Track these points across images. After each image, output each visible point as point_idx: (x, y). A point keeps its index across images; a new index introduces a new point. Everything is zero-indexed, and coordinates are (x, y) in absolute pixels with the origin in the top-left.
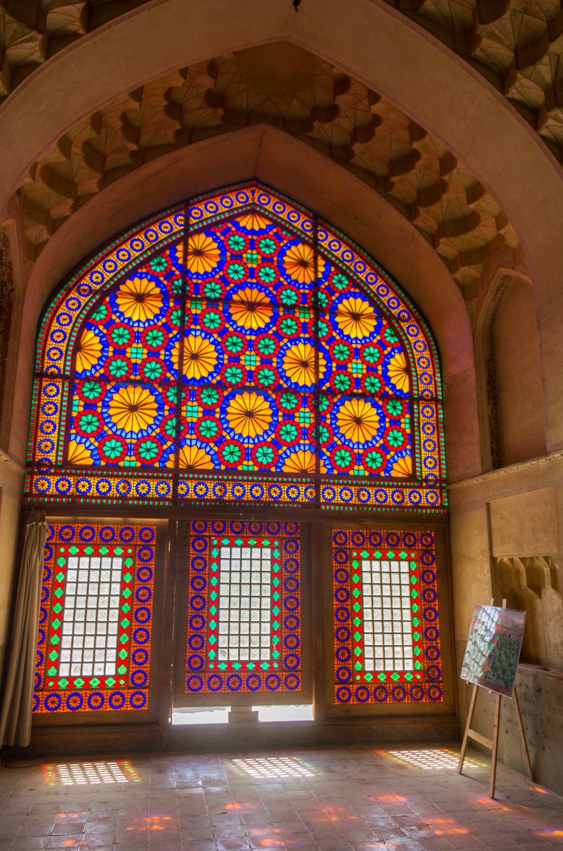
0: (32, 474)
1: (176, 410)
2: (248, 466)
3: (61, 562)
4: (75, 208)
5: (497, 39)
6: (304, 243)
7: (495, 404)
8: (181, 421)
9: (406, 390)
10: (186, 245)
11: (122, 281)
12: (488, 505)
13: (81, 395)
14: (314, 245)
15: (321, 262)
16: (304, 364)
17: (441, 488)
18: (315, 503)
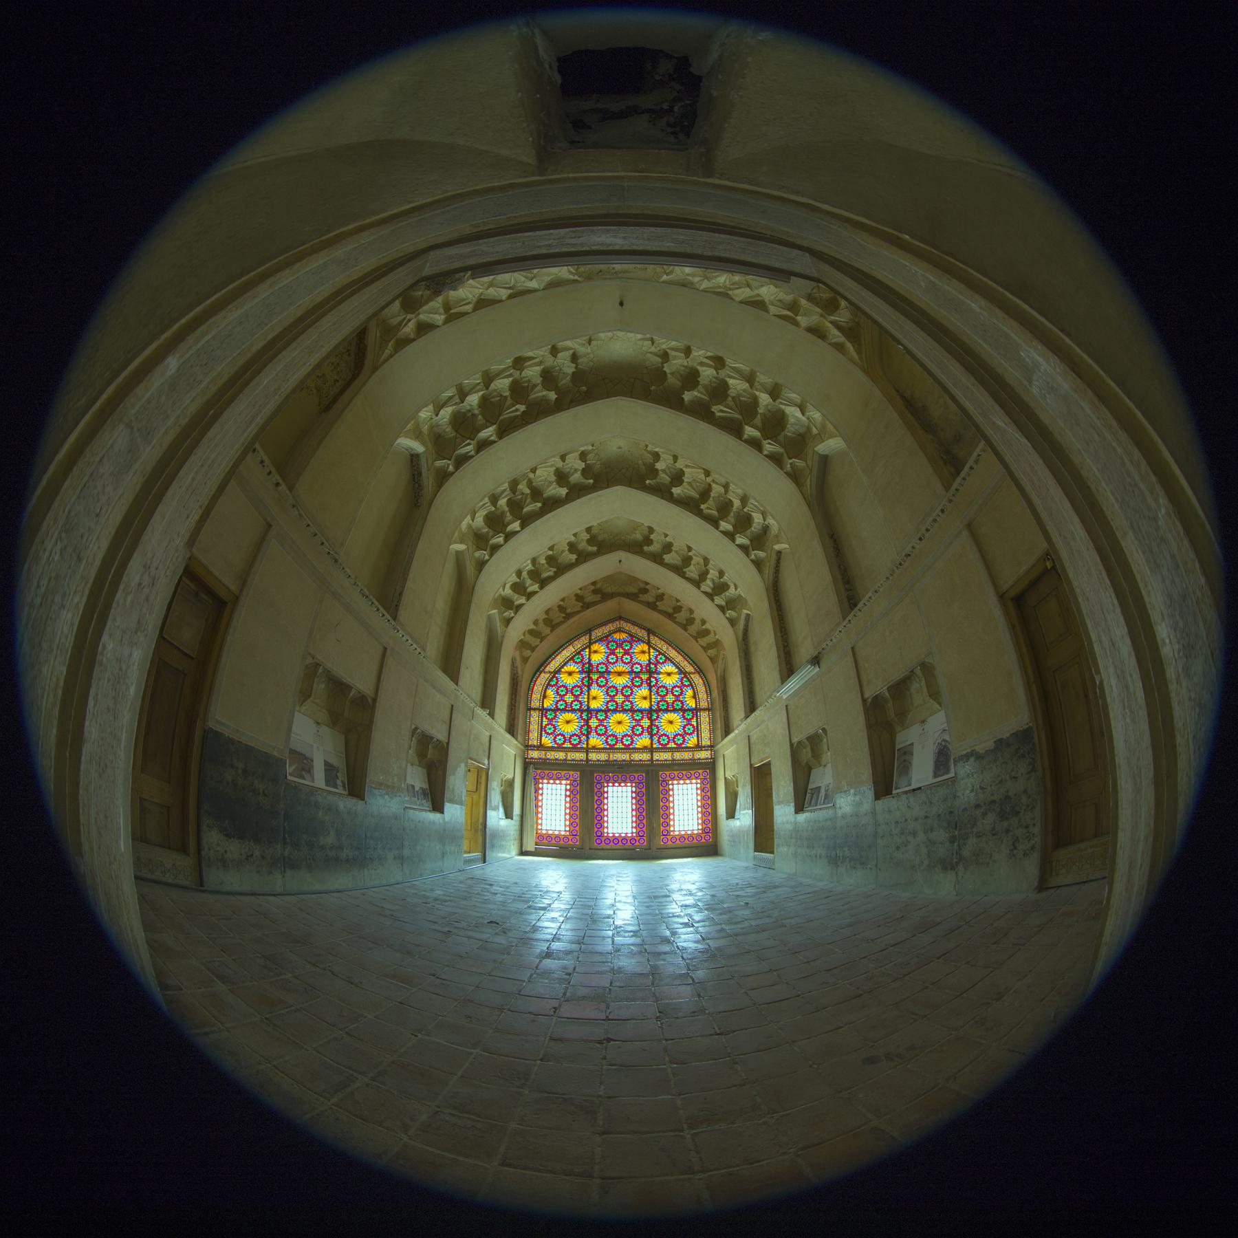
0: (528, 750)
1: (587, 721)
2: (619, 745)
3: (541, 786)
4: (541, 642)
5: (692, 572)
6: (644, 642)
7: (727, 710)
8: (589, 727)
9: (694, 706)
10: (590, 649)
11: (562, 667)
12: (724, 755)
13: (546, 717)
14: (649, 643)
15: (652, 650)
16: (645, 698)
17: (711, 750)
18: (652, 760)
